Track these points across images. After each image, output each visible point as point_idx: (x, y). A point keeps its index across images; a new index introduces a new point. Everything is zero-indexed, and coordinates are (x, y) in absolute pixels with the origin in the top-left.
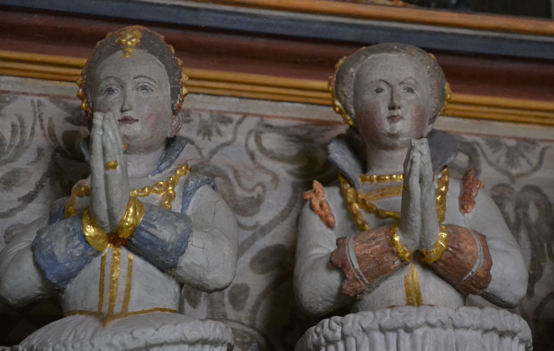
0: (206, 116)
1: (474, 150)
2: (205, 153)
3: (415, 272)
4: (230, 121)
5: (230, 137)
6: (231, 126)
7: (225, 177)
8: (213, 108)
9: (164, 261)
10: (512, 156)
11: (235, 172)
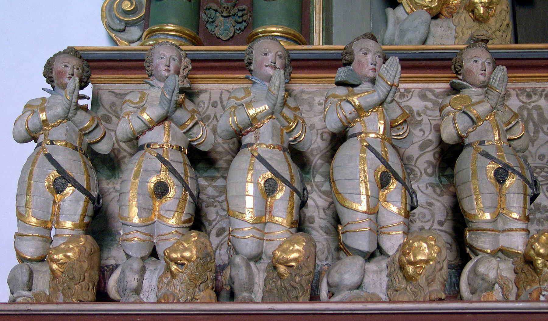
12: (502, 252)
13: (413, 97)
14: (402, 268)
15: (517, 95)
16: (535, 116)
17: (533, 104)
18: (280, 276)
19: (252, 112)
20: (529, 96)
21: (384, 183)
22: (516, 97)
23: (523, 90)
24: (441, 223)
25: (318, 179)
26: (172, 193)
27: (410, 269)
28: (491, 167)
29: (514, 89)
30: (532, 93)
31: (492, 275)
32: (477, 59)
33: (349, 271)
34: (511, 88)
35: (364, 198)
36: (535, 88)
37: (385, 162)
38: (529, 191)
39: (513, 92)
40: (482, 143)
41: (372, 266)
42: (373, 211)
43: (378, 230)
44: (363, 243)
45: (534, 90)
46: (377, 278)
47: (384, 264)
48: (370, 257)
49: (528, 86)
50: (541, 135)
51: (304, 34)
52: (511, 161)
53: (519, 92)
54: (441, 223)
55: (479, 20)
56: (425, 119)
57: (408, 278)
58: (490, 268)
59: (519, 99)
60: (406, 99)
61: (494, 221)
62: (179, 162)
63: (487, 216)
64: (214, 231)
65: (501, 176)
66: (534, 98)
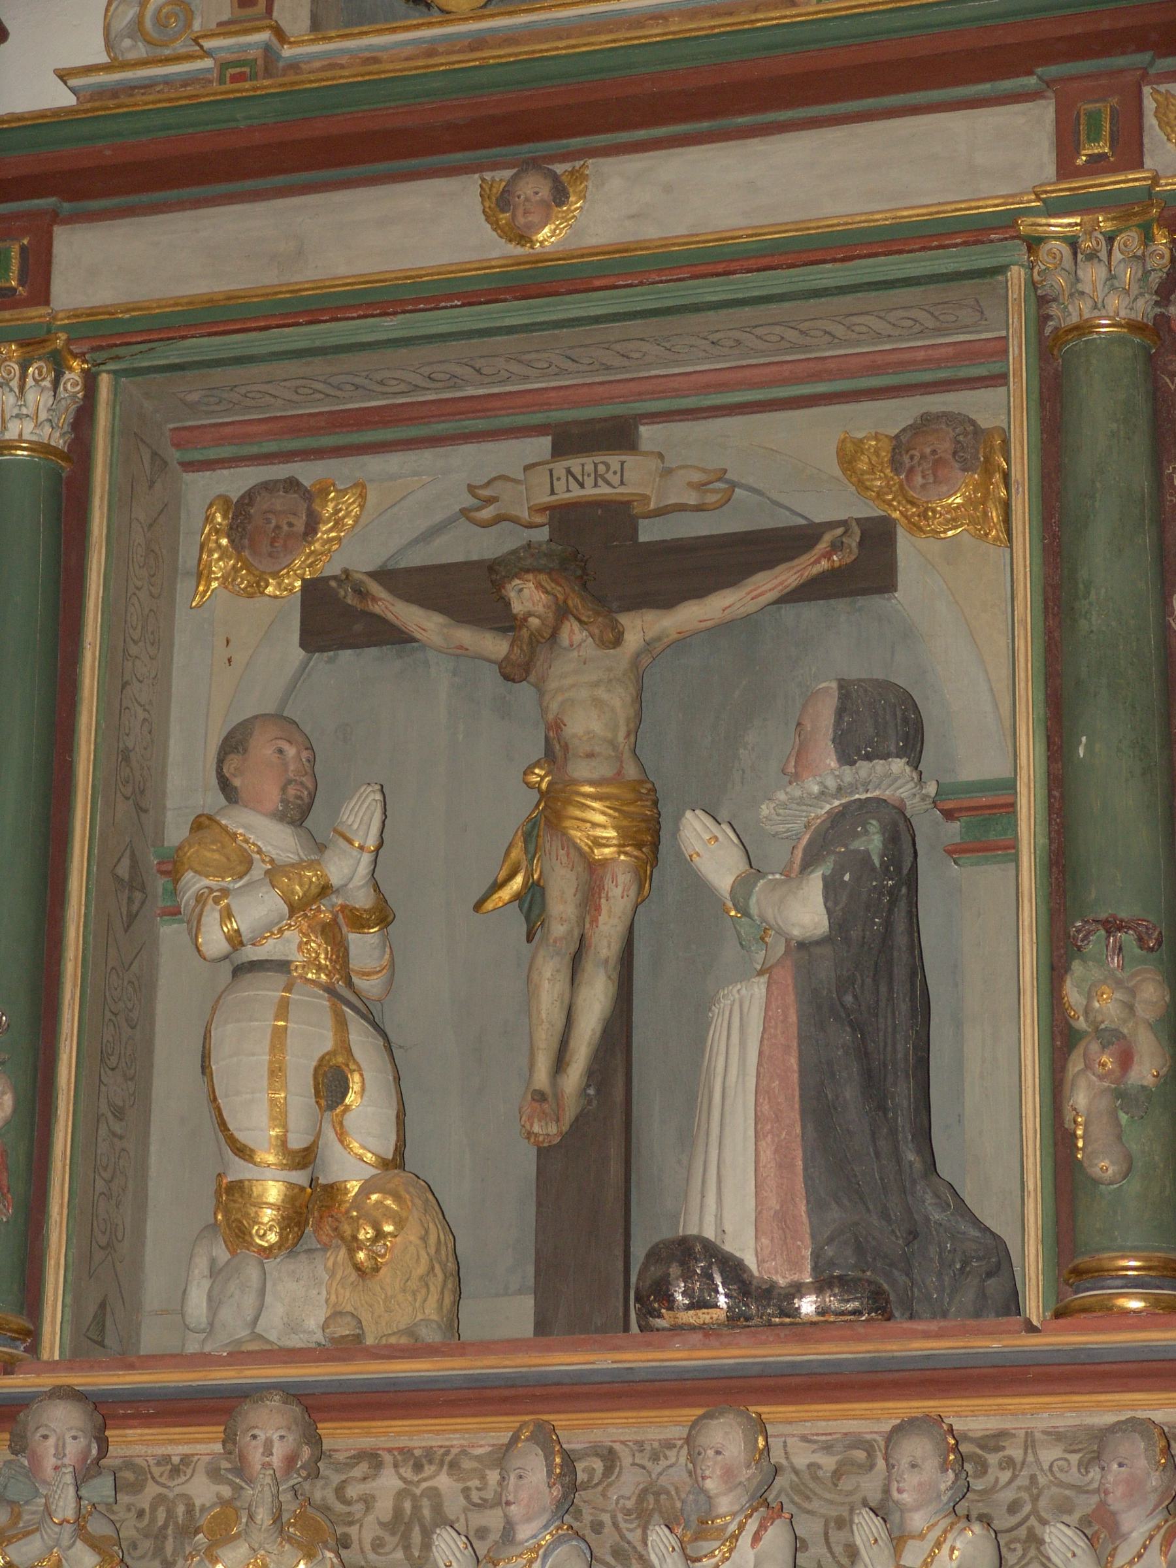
0: (656, 1445)
1: (872, 1446)
2: (654, 1476)
4: (675, 1446)
5: (673, 1460)
6: (675, 1450)
7: (668, 1493)
8: (662, 1437)
11: (677, 1489)
13: (196, 1475)
15: (396, 1466)
16: (426, 1512)
17: (425, 1485)
20: (418, 1467)
22: (393, 1470)
23: (406, 1452)
29: (390, 1450)
30: (424, 1461)
32: (256, 1432)
34: (384, 1449)
36: (431, 1447)
39: (388, 1458)
45: (429, 1453)
49: (416, 1444)
53: (399, 1458)
59: (398, 1473)
60: (183, 1479)
66: (429, 1470)
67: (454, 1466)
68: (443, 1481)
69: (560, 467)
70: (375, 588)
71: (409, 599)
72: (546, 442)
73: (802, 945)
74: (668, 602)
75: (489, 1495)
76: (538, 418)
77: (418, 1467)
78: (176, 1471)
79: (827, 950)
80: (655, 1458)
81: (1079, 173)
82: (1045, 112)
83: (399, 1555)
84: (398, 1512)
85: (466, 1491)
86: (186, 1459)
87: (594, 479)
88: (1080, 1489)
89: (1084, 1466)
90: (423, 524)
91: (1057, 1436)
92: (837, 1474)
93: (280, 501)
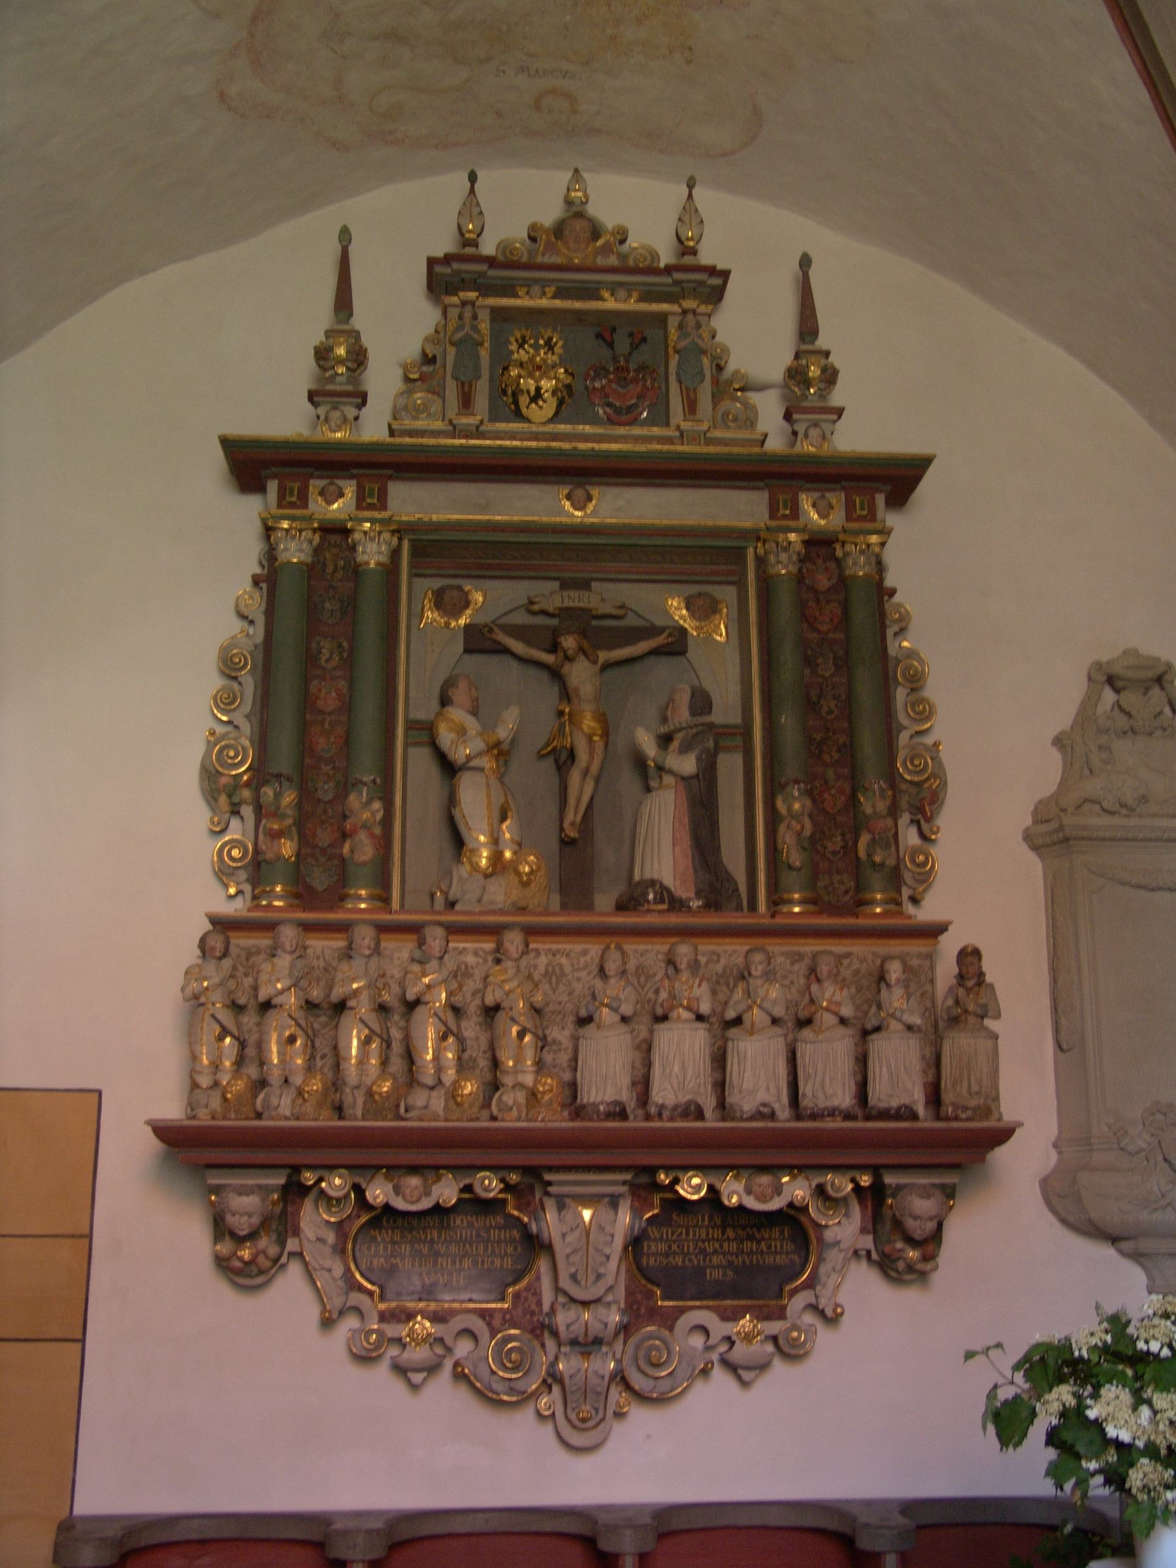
3: (681, 1010)
9: (616, 1010)
10: (730, 956)
12: (519, 1085)
14: (454, 1097)
16: (557, 971)
18: (375, 1101)
19: (355, 986)
20: (554, 955)
21: (444, 1038)
23: (550, 950)
24: (485, 1052)
25: (396, 1017)
26: (298, 1043)
27: (459, 1099)
28: (515, 1030)
31: (511, 1103)
33: (419, 1098)
35: (430, 1051)
37: (445, 1024)
38: (540, 1044)
40: (511, 1009)
41: (434, 1093)
42: (437, 1058)
43: (439, 1069)
44: (429, 1081)
45: (558, 951)
46: (437, 1102)
47: (442, 1092)
48: (432, 1088)
50: (561, 986)
51: (384, 899)
52: (529, 1025)
54: (485, 1052)
55: (525, 885)
56: (477, 972)
57: (458, 1105)
58: (509, 1098)
61: (515, 1065)
62: (300, 1015)
63: (511, 1063)
64: (318, 1056)
65: (521, 1035)
67: (568, 955)
68: (564, 960)
69: (566, 594)
70: (496, 629)
71: (511, 635)
72: (557, 584)
73: (683, 778)
74: (611, 647)
75: (581, 965)
76: (553, 575)
77: (554, 955)
78: (460, 953)
79: (695, 782)
80: (642, 955)
81: (778, 519)
82: (765, 495)
83: (547, 985)
84: (547, 971)
85: (573, 965)
86: (465, 949)
87: (574, 599)
88: (790, 972)
89: (792, 963)
90: (508, 608)
91: (783, 954)
92: (707, 963)
93: (455, 593)
